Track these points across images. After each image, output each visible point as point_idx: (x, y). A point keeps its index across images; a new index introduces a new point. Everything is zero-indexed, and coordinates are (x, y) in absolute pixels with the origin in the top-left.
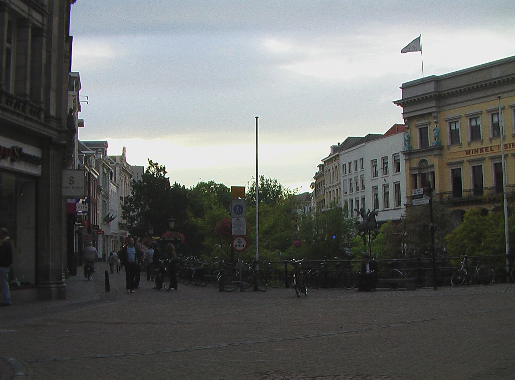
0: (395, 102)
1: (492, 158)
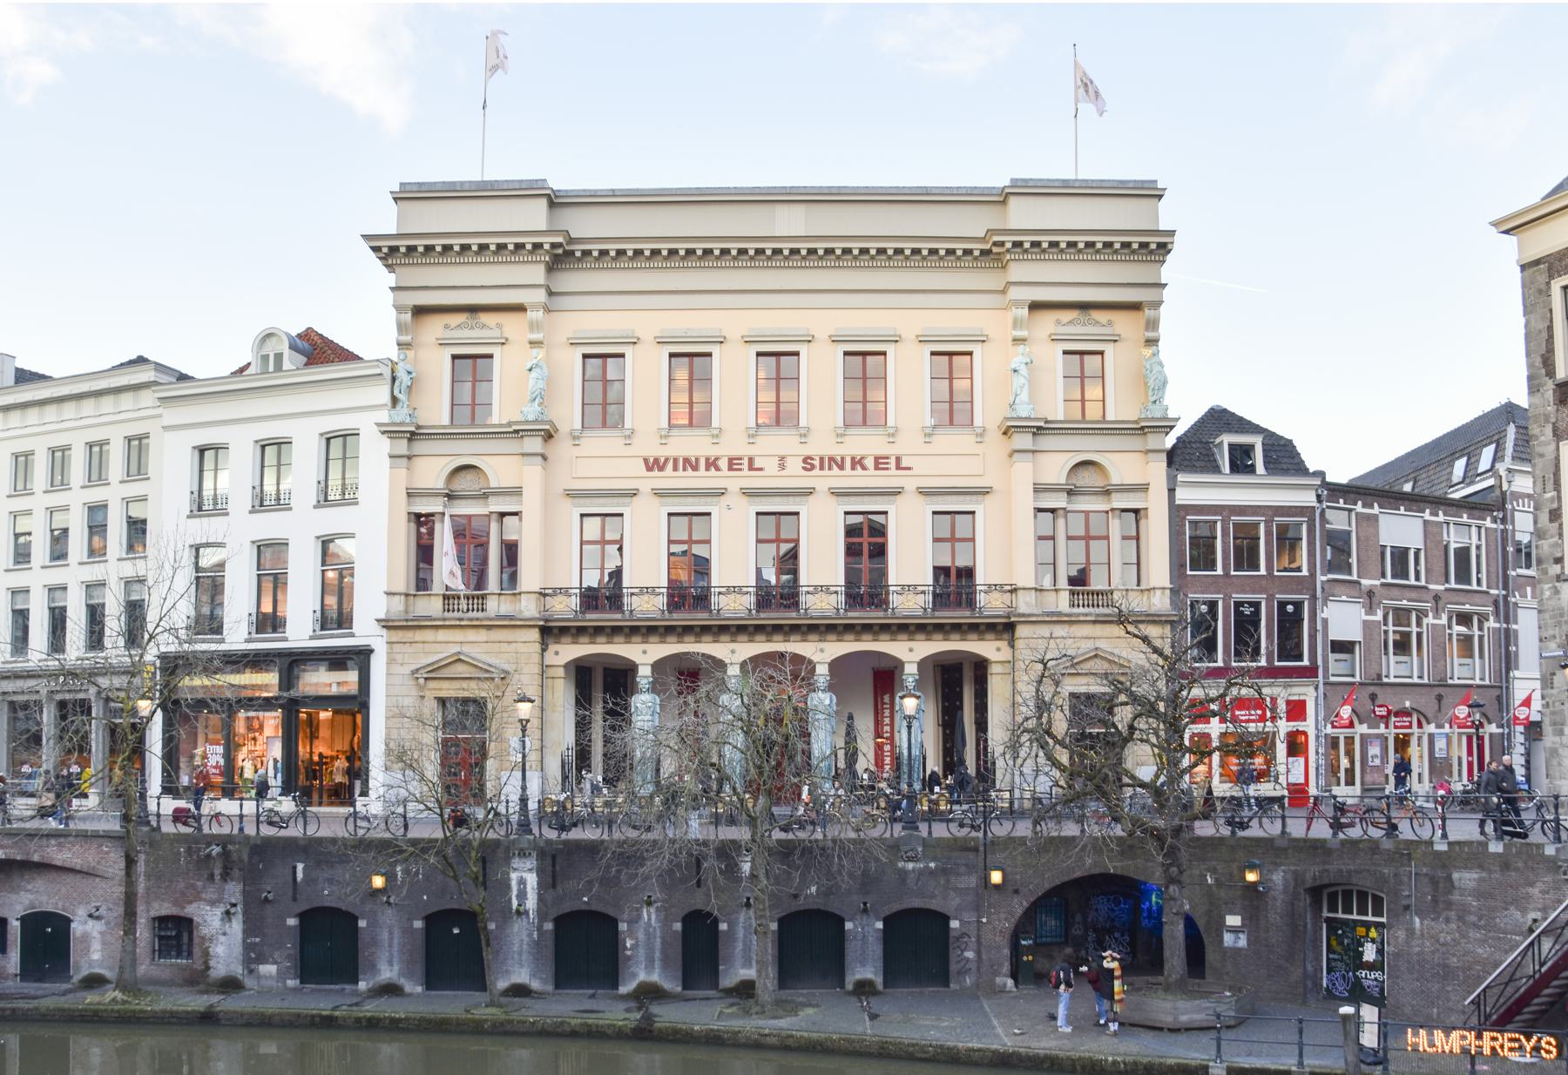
0: (366, 237)
1: (750, 493)
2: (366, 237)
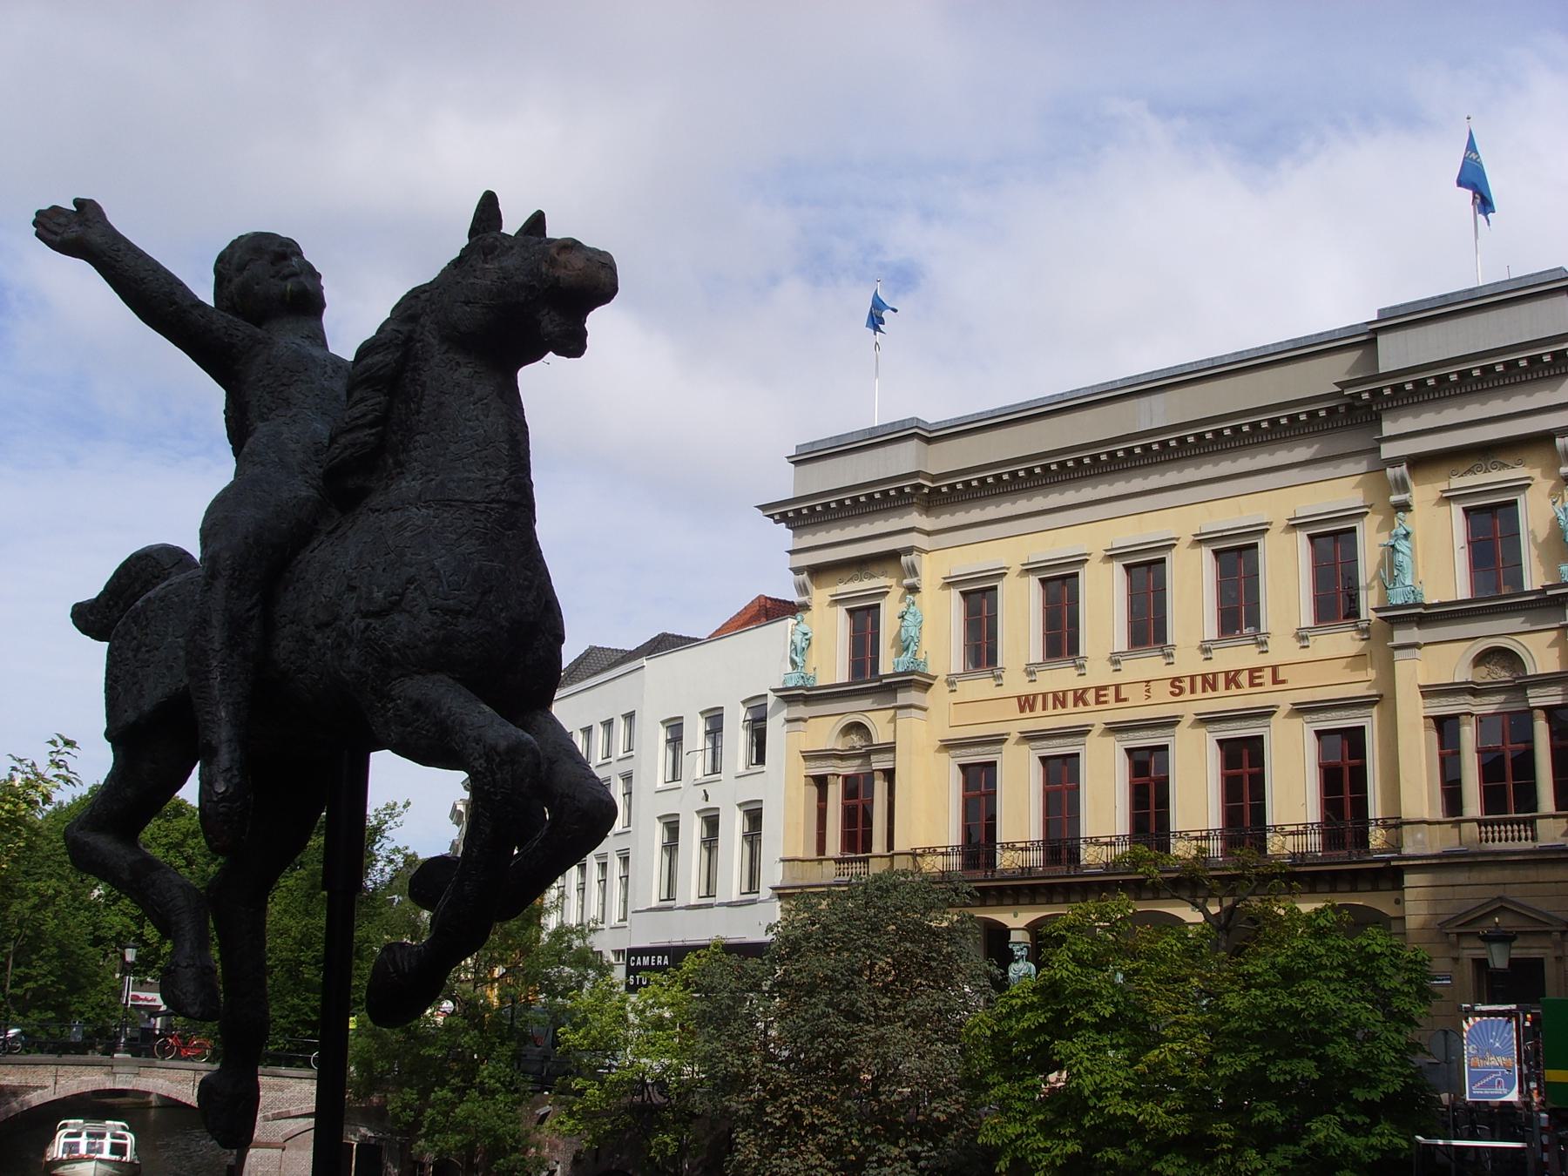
0: (762, 507)
1: (1115, 729)
2: (762, 507)
